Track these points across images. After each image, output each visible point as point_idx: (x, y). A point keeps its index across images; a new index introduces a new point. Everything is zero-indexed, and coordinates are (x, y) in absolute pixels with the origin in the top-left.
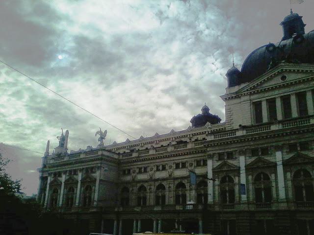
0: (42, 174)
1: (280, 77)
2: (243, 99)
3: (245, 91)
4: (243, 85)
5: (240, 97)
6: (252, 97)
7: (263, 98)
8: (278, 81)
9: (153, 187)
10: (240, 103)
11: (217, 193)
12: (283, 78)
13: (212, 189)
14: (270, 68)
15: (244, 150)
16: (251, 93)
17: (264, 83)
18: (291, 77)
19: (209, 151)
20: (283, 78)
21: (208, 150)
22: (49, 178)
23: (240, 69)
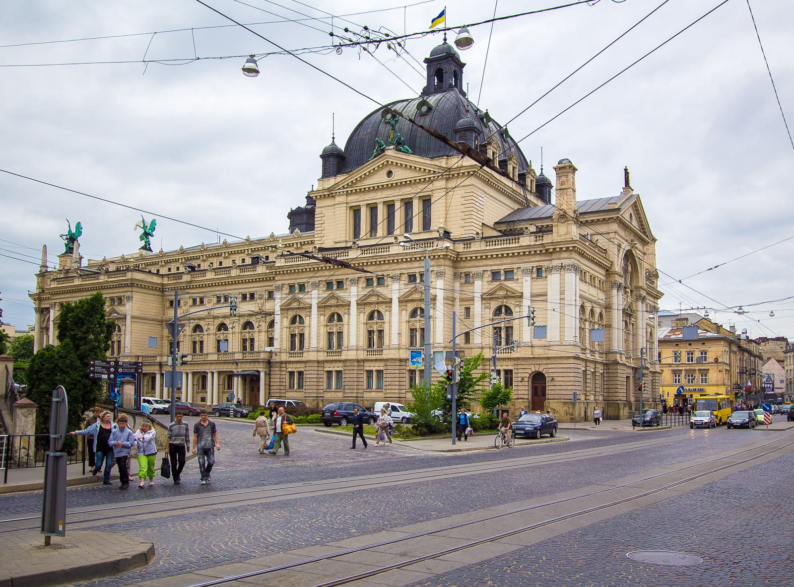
0: (39, 304)
1: (384, 172)
2: (339, 199)
3: (339, 189)
4: (340, 178)
5: (334, 197)
6: (351, 198)
7: (362, 200)
8: (381, 178)
9: (211, 327)
10: (334, 205)
11: (284, 337)
12: (390, 173)
13: (281, 332)
14: (375, 157)
15: (317, 282)
16: (347, 191)
17: (364, 179)
18: (399, 175)
19: (277, 281)
20: (390, 173)
21: (276, 278)
22: (52, 311)
23: (341, 145)
